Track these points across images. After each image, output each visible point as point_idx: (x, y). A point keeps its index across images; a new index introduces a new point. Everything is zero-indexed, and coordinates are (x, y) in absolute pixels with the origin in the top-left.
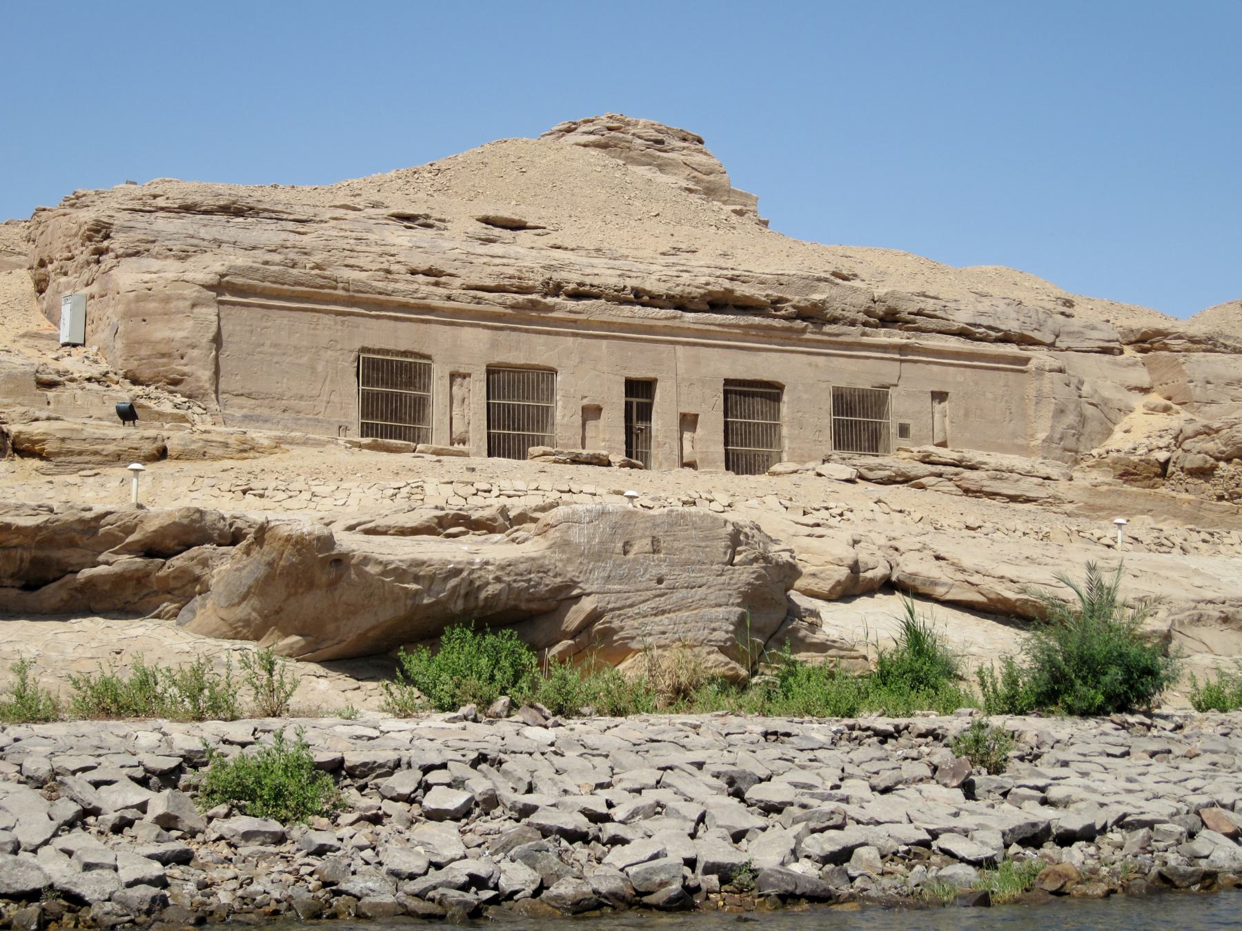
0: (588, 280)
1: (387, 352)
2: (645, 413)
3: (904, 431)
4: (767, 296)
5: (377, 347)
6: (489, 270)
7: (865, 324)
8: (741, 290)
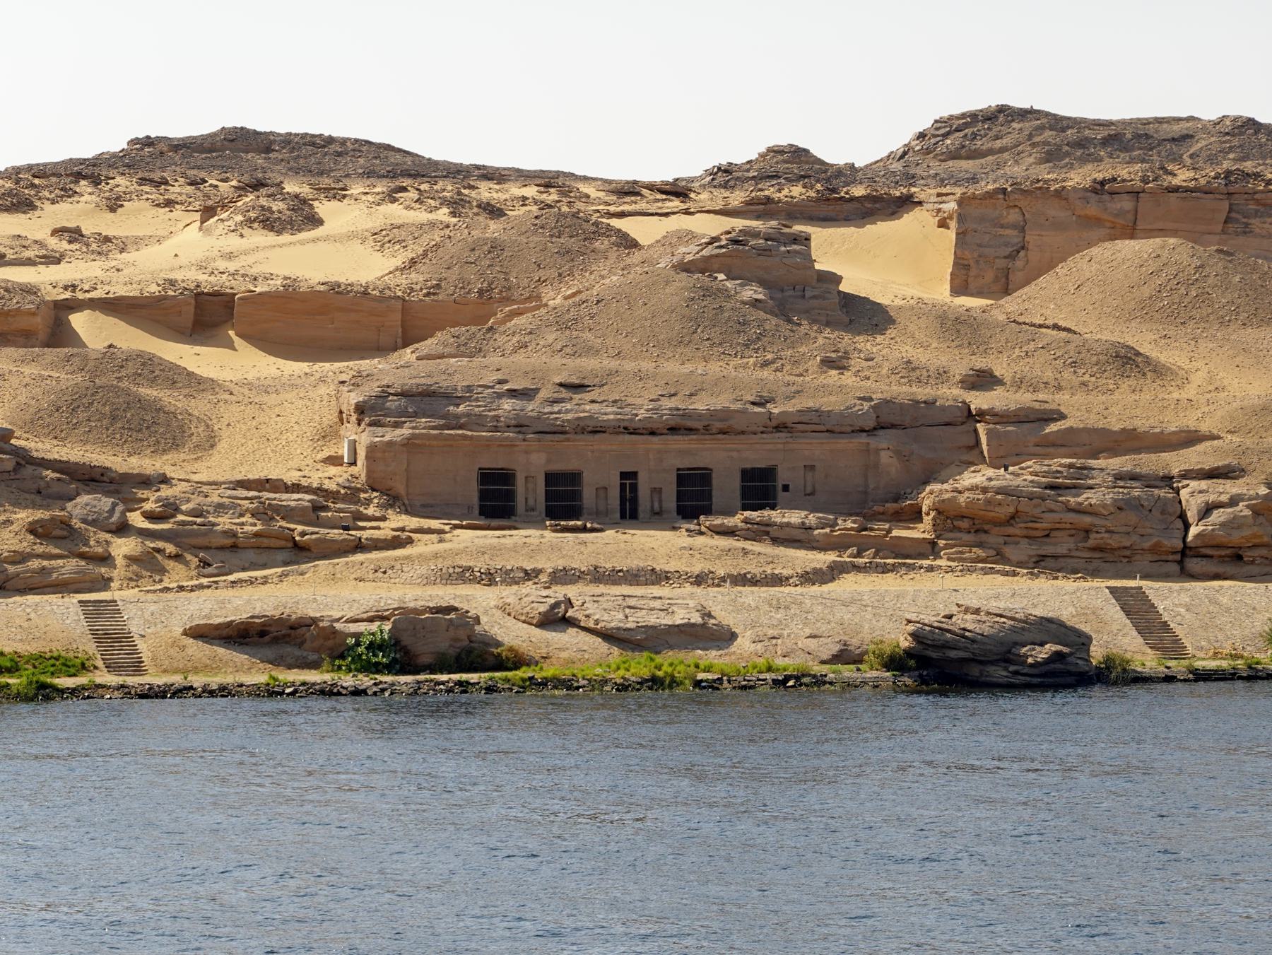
2: (634, 488)
3: (786, 488)
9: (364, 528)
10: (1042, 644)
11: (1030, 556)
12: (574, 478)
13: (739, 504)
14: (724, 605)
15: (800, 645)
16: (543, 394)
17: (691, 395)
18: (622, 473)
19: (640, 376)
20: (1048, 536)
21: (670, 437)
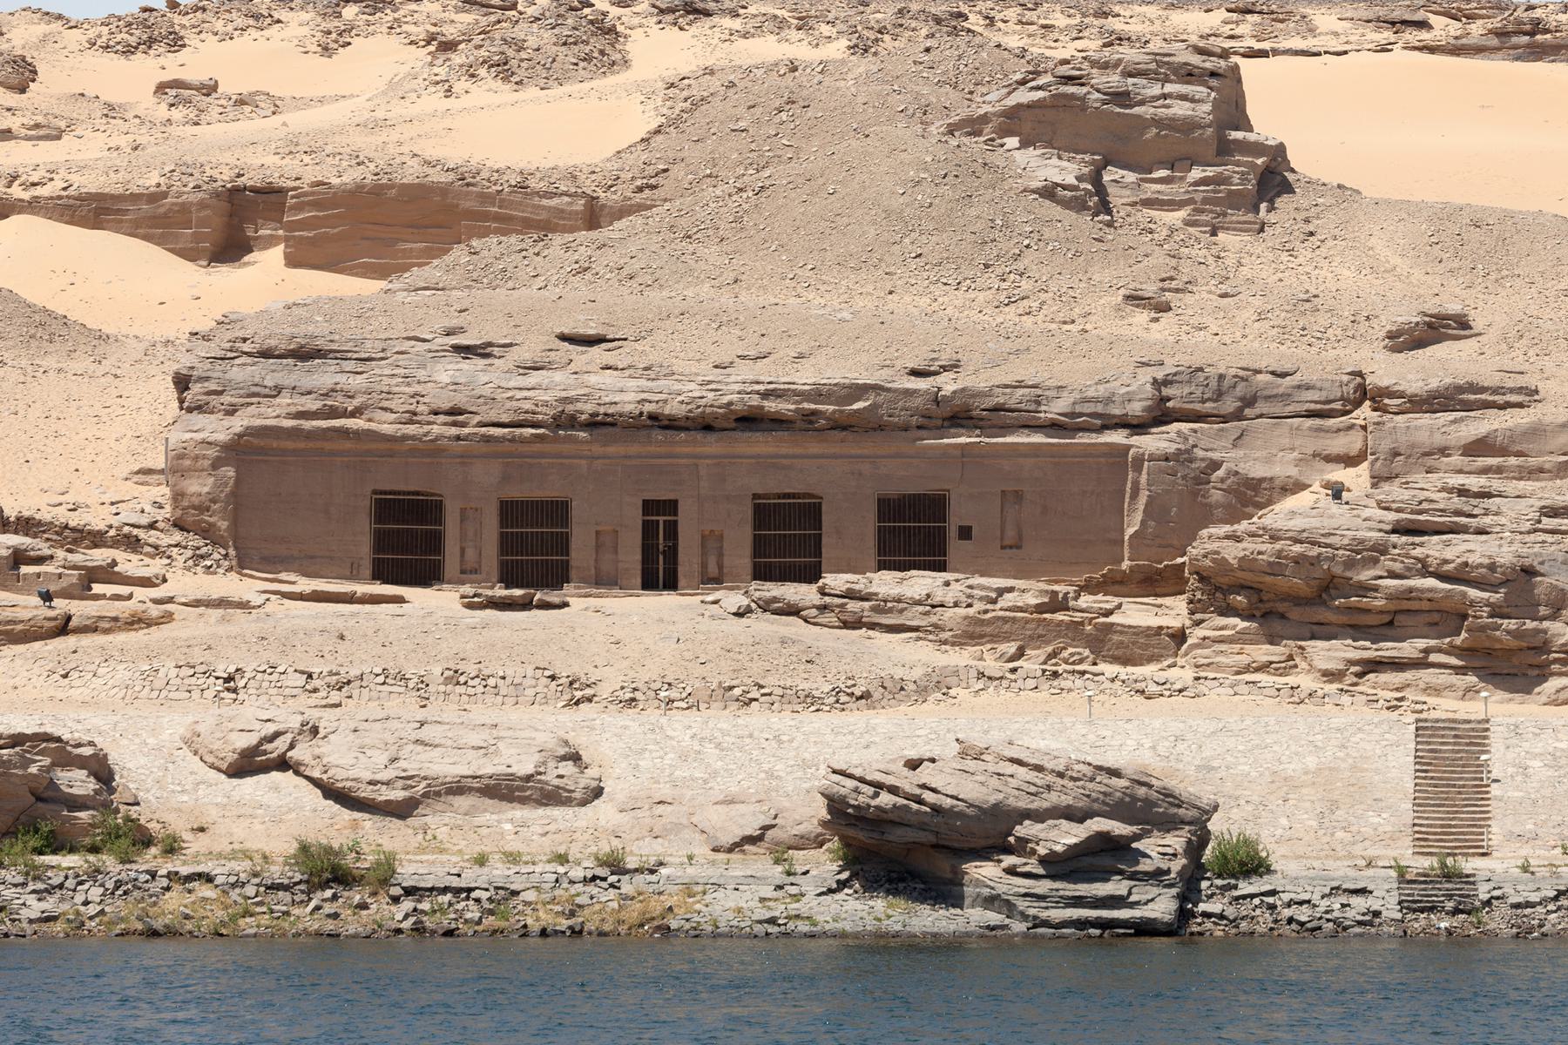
0: (602, 410)
1: (399, 493)
2: (672, 530)
3: (965, 533)
4: (796, 410)
5: (388, 488)
6: (509, 404)
7: (919, 427)
8: (771, 406)
9: (97, 597)
10: (1081, 821)
11: (1352, 663)
12: (558, 511)
13: (874, 564)
14: (609, 739)
15: (694, 820)
16: (515, 355)
17: (801, 356)
18: (646, 503)
19: (722, 321)
20: (1391, 623)
21: (738, 434)
